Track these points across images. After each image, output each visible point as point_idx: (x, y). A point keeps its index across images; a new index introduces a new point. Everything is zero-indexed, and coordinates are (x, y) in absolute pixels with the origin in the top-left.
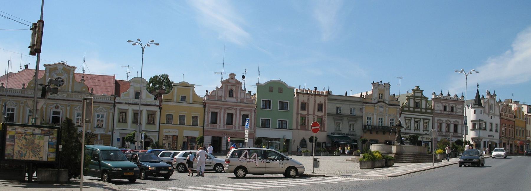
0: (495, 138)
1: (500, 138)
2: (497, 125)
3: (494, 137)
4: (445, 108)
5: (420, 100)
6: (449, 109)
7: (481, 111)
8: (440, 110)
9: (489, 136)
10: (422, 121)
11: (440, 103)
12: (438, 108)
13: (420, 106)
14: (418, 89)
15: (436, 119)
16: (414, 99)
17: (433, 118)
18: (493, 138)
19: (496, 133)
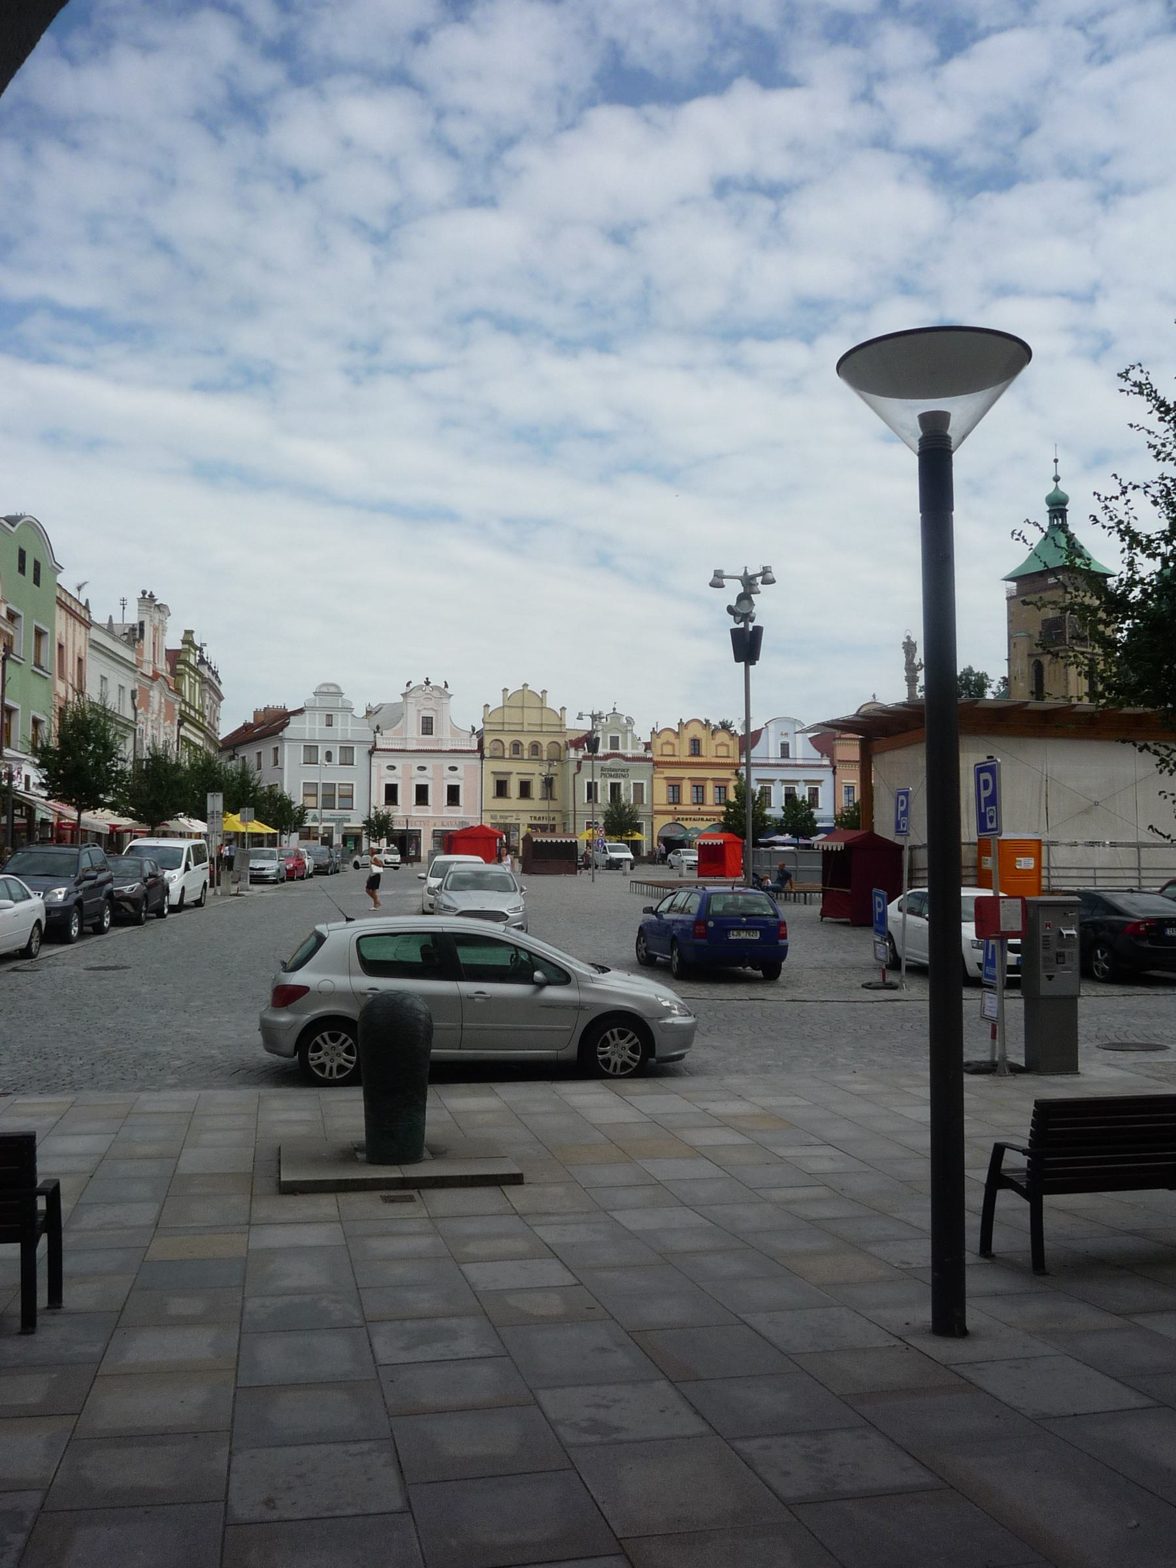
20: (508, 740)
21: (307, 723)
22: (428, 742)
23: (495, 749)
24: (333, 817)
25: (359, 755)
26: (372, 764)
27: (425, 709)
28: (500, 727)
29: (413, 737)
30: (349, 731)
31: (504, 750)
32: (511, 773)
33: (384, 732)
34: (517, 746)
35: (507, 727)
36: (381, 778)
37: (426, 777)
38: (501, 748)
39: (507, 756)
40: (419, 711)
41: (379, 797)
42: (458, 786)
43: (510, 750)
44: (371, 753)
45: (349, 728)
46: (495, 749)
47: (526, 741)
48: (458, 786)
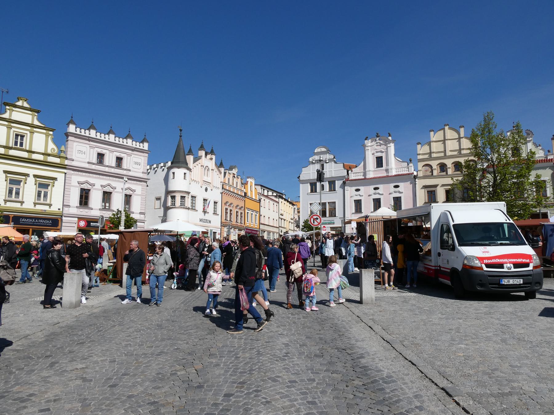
0: (212, 224)
1: (221, 224)
2: (215, 203)
3: (210, 222)
4: (101, 156)
5: (28, 132)
6: (110, 159)
7: (185, 174)
8: (88, 161)
9: (201, 220)
10: (31, 180)
11: (88, 146)
12: (83, 156)
13: (26, 146)
14: (23, 103)
15: (76, 179)
16: (9, 128)
17: (67, 176)
18: (209, 224)
19: (215, 216)
20: (435, 164)
21: (311, 170)
22: (381, 173)
23: (426, 171)
24: (325, 222)
25: (338, 184)
26: (346, 189)
27: (377, 152)
28: (426, 156)
29: (372, 171)
30: (333, 172)
31: (432, 172)
32: (437, 185)
33: (353, 169)
34: (443, 167)
35: (434, 155)
36: (351, 197)
37: (379, 194)
38: (430, 170)
39: (435, 173)
40: (373, 154)
41: (351, 207)
42: (401, 197)
43: (438, 170)
44: (344, 183)
45: (333, 170)
46: (426, 171)
47: (449, 163)
48: (401, 197)
